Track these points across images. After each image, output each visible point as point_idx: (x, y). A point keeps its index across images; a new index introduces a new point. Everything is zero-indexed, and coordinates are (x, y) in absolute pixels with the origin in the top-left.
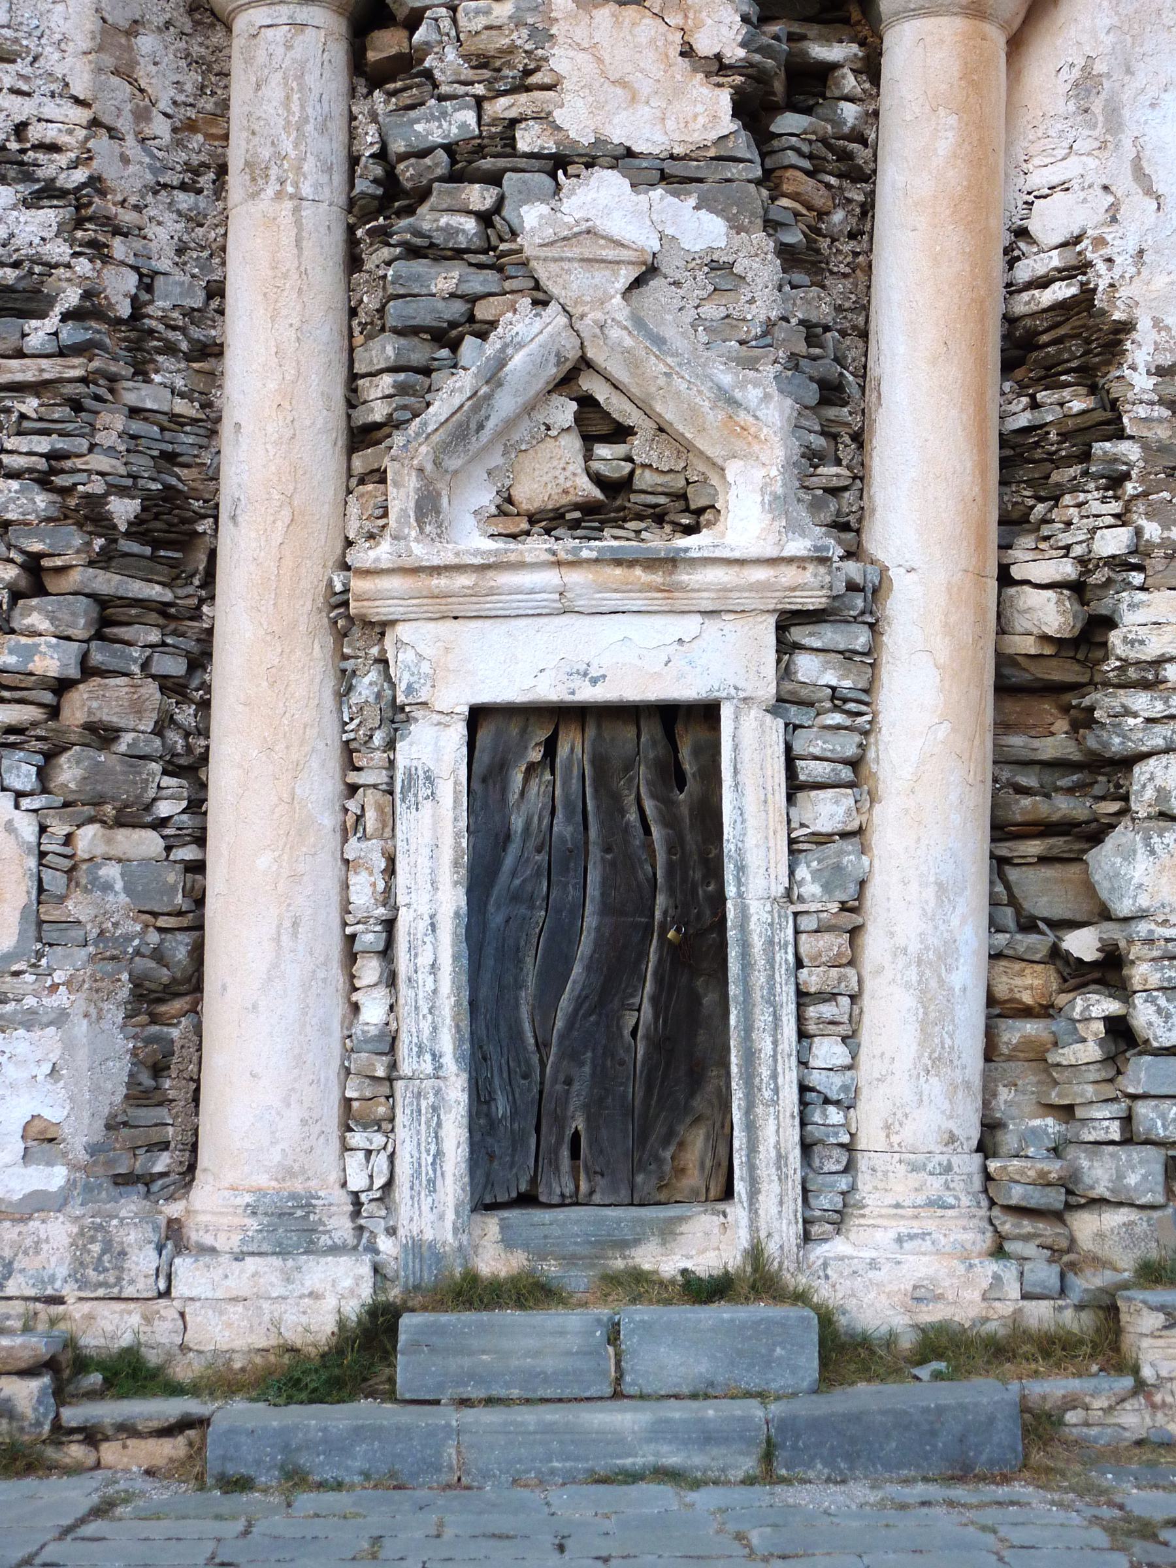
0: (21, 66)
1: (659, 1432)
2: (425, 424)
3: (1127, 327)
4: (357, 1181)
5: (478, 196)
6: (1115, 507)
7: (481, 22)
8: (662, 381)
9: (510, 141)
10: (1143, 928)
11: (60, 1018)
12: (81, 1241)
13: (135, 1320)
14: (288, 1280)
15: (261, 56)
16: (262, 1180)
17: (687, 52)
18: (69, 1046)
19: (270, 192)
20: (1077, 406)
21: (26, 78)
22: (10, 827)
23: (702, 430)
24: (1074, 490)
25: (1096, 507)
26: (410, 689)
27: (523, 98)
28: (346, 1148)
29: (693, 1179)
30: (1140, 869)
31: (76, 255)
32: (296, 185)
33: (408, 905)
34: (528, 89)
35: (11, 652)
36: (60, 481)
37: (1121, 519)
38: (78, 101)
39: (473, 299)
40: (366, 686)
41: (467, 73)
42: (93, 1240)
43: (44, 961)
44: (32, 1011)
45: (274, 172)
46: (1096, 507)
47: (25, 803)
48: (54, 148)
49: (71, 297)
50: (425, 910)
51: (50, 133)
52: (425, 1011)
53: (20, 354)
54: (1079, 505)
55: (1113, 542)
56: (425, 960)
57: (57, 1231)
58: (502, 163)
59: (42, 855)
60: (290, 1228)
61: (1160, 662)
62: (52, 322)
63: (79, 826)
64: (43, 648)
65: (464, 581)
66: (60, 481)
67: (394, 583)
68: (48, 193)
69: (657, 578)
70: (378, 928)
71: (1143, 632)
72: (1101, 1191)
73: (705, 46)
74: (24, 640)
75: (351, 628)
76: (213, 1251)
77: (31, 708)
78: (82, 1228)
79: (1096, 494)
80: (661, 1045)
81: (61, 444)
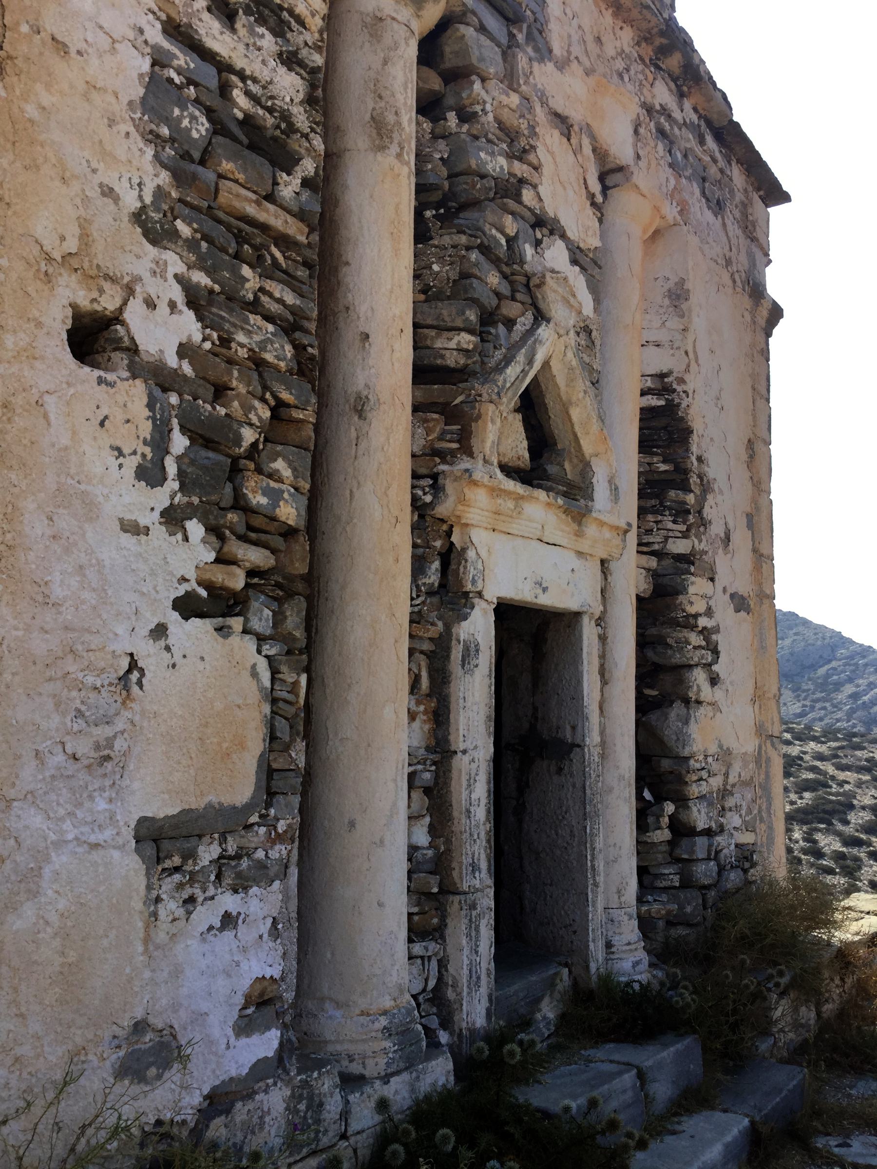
2: (505, 381)
5: (511, 226)
8: (581, 395)
10: (692, 762)
20: (663, 467)
22: (254, 673)
23: (587, 433)
25: (670, 525)
31: (313, 130)
32: (408, 154)
33: (464, 752)
35: (264, 494)
37: (685, 535)
42: (300, 1098)
43: (272, 812)
44: (261, 866)
46: (670, 525)
47: (267, 649)
52: (476, 837)
54: (657, 522)
55: (679, 547)
57: (275, 1100)
59: (274, 701)
61: (696, 616)
63: (298, 675)
64: (286, 495)
70: (433, 768)
71: (693, 599)
74: (273, 484)
77: (267, 553)
78: (293, 1091)
79: (670, 518)
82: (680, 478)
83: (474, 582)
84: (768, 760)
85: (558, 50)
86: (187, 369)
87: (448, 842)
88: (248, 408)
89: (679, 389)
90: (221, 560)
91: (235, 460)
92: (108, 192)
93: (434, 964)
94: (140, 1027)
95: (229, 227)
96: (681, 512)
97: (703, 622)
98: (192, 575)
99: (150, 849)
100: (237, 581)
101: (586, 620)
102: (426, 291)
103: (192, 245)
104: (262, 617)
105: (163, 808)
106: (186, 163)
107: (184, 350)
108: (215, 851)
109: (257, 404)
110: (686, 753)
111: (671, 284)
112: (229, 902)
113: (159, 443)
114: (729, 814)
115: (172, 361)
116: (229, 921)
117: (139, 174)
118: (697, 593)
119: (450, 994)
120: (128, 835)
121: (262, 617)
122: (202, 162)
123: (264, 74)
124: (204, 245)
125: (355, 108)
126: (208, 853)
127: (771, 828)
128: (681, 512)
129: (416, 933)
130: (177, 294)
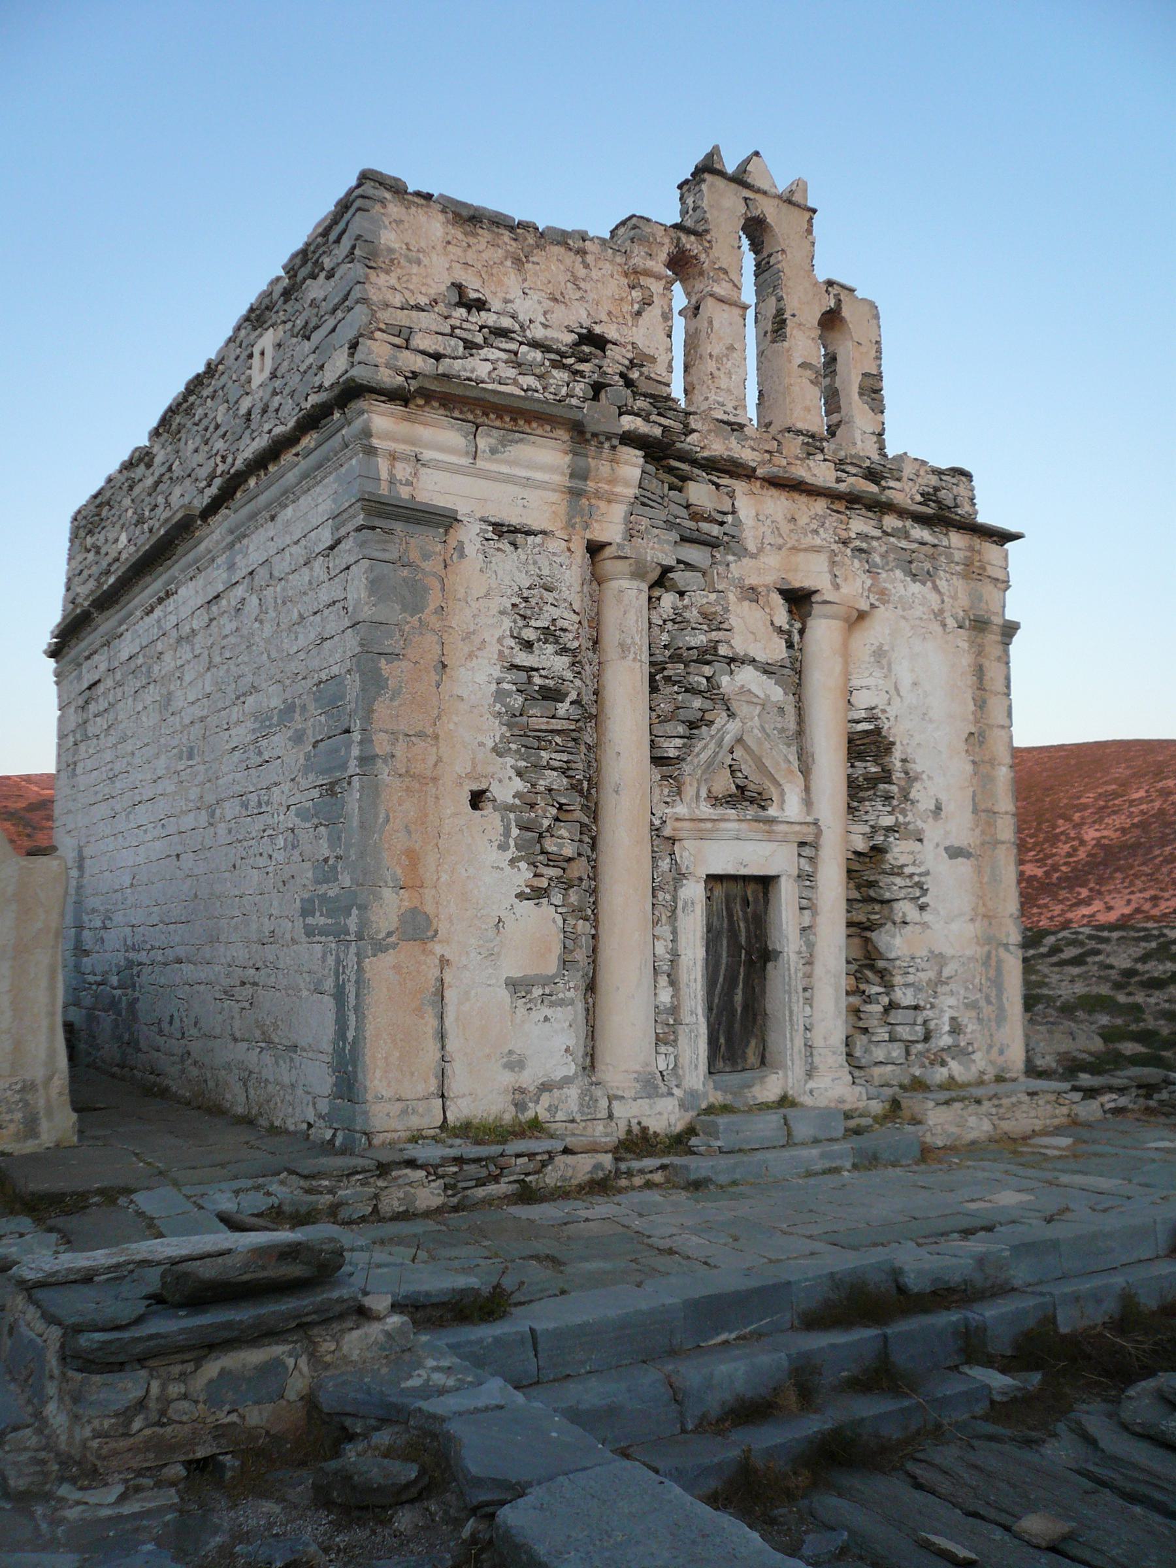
0: (554, 594)
1: (823, 1156)
3: (893, 743)
4: (662, 1067)
5: (707, 670)
6: (889, 809)
7: (705, 601)
9: (715, 648)
10: (898, 963)
11: (572, 1002)
12: (582, 1096)
13: (601, 1128)
14: (651, 1108)
15: (626, 602)
16: (638, 1068)
17: (772, 624)
18: (575, 1011)
19: (631, 656)
20: (873, 770)
21: (556, 599)
22: (554, 921)
24: (871, 800)
25: (881, 808)
26: (687, 868)
27: (721, 633)
28: (657, 1053)
29: (752, 1059)
30: (898, 941)
34: (720, 629)
36: (571, 773)
37: (890, 813)
38: (574, 612)
39: (704, 711)
40: (665, 864)
41: (701, 620)
44: (562, 999)
45: (632, 650)
46: (881, 808)
48: (564, 630)
49: (573, 696)
50: (692, 957)
51: (565, 624)
53: (553, 717)
55: (888, 821)
56: (692, 977)
57: (573, 1093)
58: (714, 658)
60: (651, 1086)
61: (903, 866)
62: (566, 705)
65: (709, 825)
66: (571, 773)
67: (687, 825)
68: (564, 650)
69: (766, 827)
71: (898, 855)
72: (881, 1059)
73: (778, 624)
75: (662, 840)
76: (623, 1097)
80: (746, 1007)
81: (571, 757)
82: (886, 776)
83: (687, 868)
84: (999, 962)
85: (752, 547)
86: (517, 802)
87: (678, 1000)
88: (545, 811)
89: (882, 716)
90: (536, 875)
91: (541, 834)
92: (481, 744)
93: (672, 1057)
94: (510, 1052)
95: (534, 737)
96: (888, 798)
97: (907, 870)
98: (523, 884)
99: (511, 988)
100: (544, 883)
101: (783, 880)
102: (657, 719)
103: (518, 751)
104: (557, 899)
105: (517, 974)
106: (513, 718)
107: (514, 797)
108: (540, 992)
109: (550, 808)
110: (892, 956)
111: (874, 648)
112: (548, 1012)
113: (507, 833)
114: (942, 998)
115: (511, 801)
116: (546, 1019)
117: (494, 731)
118: (900, 851)
119: (680, 1072)
120: (502, 982)
121: (557, 899)
122: (521, 715)
123: (547, 665)
124: (523, 750)
125: (611, 638)
126: (537, 992)
127: (1001, 1008)
128: (888, 798)
129: (659, 1040)
130: (512, 773)
